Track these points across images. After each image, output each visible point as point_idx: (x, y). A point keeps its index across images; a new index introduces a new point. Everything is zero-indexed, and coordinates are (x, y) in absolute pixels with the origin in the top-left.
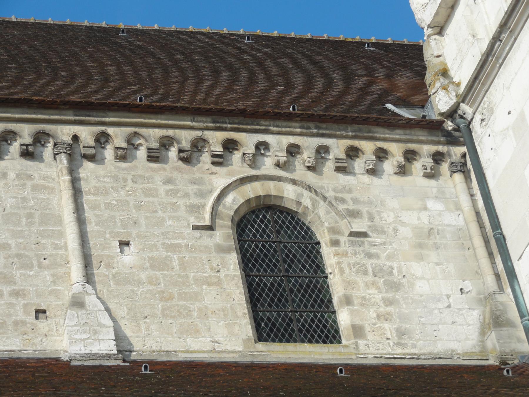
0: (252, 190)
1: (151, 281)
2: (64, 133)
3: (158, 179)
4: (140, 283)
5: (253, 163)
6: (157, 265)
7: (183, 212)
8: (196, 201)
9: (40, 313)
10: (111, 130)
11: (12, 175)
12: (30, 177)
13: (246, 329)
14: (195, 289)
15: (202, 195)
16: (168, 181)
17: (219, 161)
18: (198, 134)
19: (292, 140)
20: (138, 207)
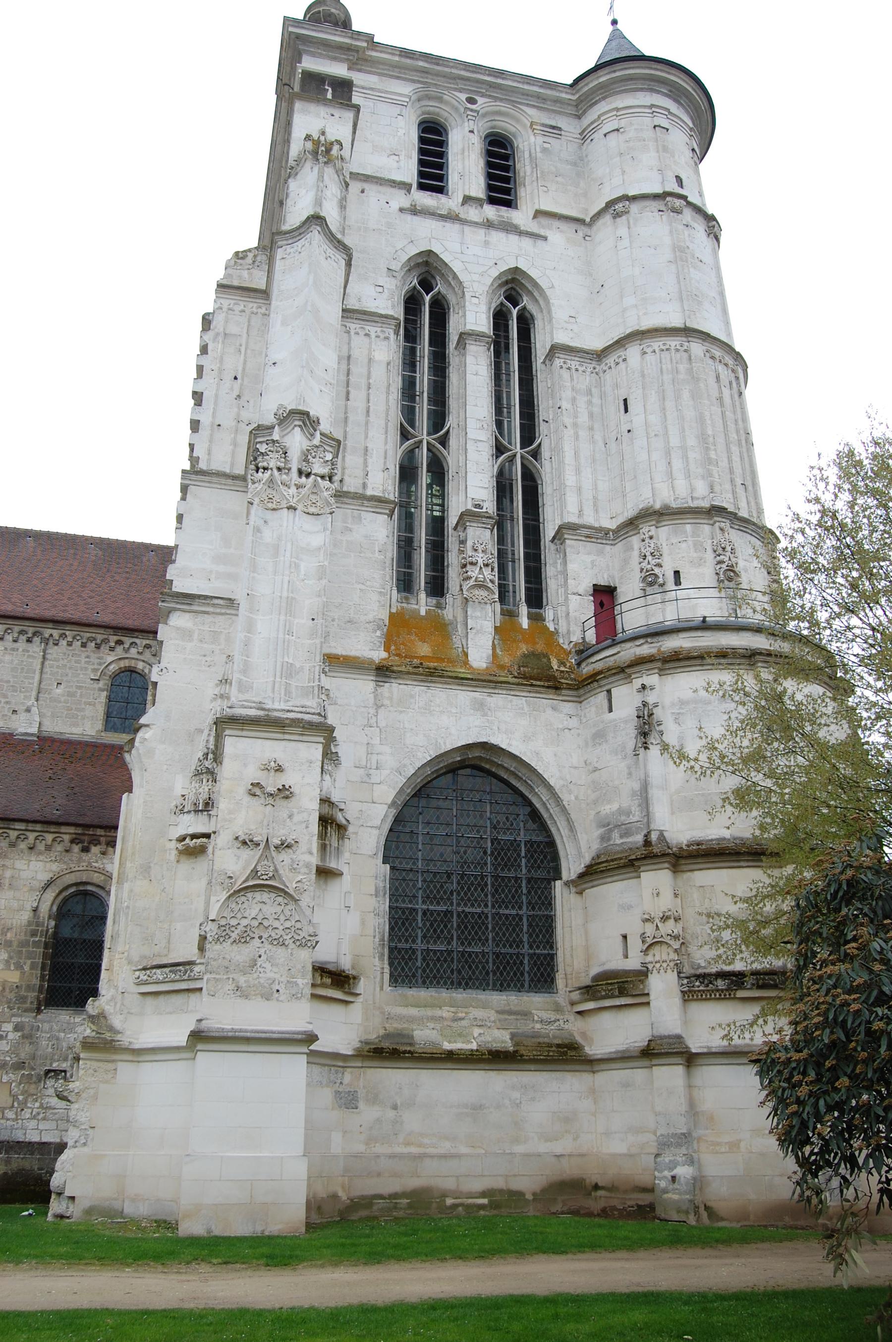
0: (122, 664)
1: (66, 702)
2: (47, 633)
3: (83, 655)
4: (60, 702)
5: (127, 651)
6: (71, 694)
7: (89, 672)
8: (96, 667)
9: (14, 711)
10: (67, 633)
11: (21, 650)
12: (28, 651)
13: (99, 725)
14: (83, 706)
15: (100, 664)
16: (88, 657)
17: (112, 649)
18: (106, 636)
19: (148, 642)
20: (70, 668)
